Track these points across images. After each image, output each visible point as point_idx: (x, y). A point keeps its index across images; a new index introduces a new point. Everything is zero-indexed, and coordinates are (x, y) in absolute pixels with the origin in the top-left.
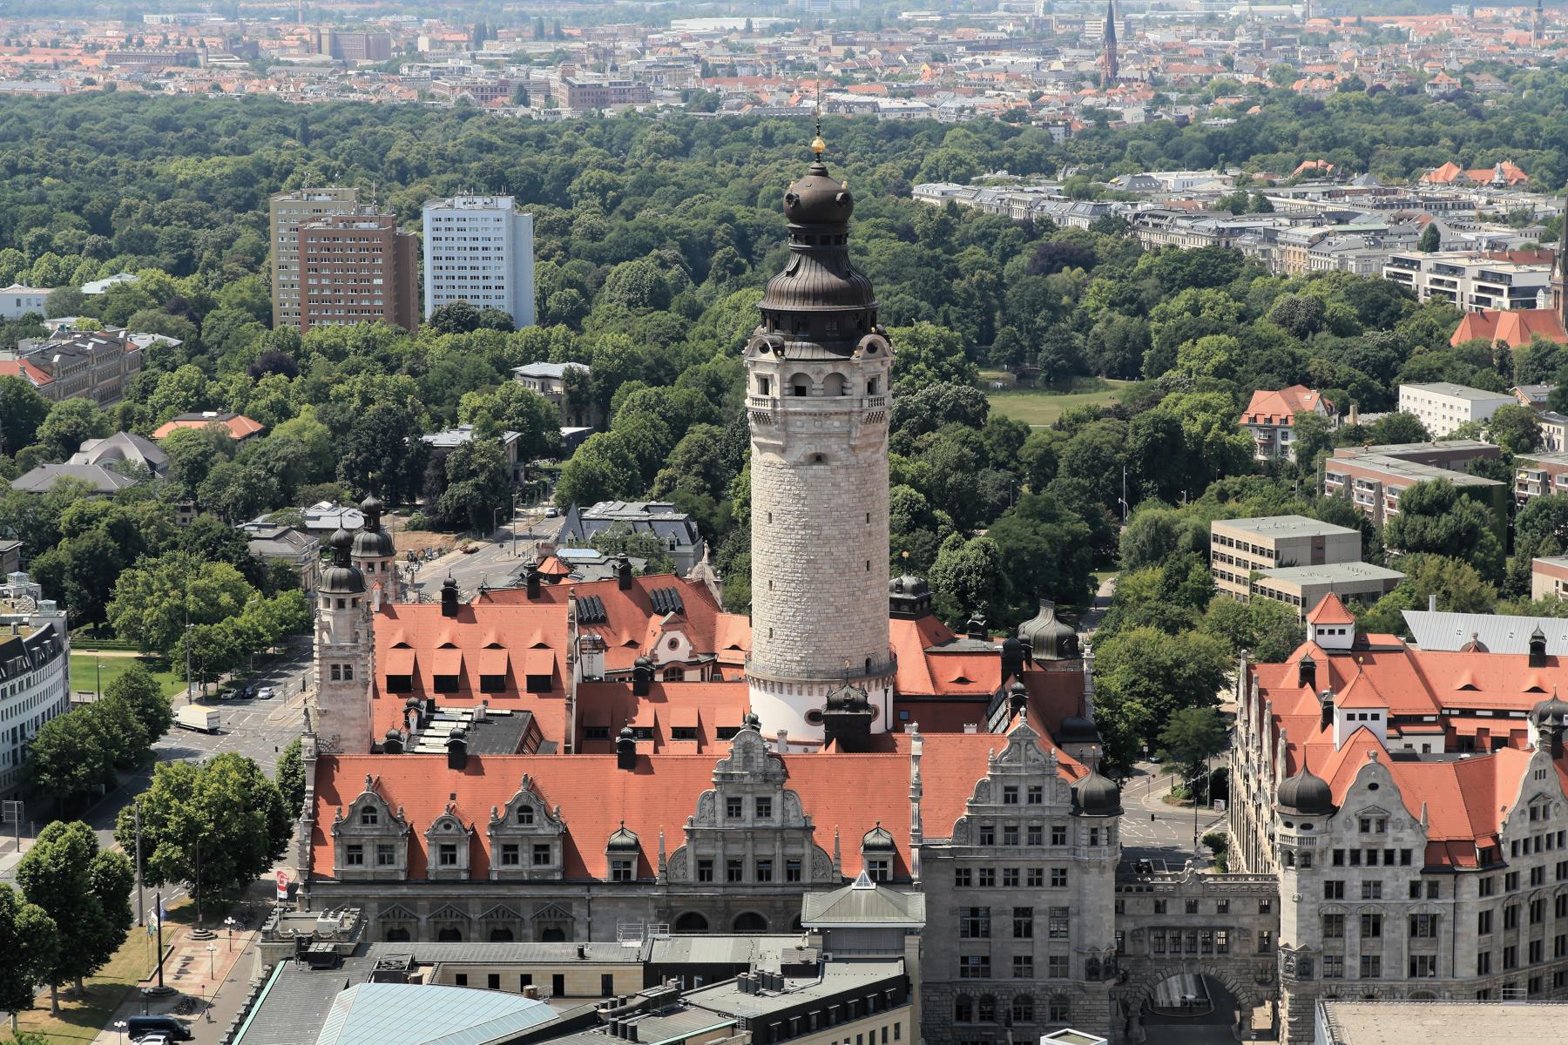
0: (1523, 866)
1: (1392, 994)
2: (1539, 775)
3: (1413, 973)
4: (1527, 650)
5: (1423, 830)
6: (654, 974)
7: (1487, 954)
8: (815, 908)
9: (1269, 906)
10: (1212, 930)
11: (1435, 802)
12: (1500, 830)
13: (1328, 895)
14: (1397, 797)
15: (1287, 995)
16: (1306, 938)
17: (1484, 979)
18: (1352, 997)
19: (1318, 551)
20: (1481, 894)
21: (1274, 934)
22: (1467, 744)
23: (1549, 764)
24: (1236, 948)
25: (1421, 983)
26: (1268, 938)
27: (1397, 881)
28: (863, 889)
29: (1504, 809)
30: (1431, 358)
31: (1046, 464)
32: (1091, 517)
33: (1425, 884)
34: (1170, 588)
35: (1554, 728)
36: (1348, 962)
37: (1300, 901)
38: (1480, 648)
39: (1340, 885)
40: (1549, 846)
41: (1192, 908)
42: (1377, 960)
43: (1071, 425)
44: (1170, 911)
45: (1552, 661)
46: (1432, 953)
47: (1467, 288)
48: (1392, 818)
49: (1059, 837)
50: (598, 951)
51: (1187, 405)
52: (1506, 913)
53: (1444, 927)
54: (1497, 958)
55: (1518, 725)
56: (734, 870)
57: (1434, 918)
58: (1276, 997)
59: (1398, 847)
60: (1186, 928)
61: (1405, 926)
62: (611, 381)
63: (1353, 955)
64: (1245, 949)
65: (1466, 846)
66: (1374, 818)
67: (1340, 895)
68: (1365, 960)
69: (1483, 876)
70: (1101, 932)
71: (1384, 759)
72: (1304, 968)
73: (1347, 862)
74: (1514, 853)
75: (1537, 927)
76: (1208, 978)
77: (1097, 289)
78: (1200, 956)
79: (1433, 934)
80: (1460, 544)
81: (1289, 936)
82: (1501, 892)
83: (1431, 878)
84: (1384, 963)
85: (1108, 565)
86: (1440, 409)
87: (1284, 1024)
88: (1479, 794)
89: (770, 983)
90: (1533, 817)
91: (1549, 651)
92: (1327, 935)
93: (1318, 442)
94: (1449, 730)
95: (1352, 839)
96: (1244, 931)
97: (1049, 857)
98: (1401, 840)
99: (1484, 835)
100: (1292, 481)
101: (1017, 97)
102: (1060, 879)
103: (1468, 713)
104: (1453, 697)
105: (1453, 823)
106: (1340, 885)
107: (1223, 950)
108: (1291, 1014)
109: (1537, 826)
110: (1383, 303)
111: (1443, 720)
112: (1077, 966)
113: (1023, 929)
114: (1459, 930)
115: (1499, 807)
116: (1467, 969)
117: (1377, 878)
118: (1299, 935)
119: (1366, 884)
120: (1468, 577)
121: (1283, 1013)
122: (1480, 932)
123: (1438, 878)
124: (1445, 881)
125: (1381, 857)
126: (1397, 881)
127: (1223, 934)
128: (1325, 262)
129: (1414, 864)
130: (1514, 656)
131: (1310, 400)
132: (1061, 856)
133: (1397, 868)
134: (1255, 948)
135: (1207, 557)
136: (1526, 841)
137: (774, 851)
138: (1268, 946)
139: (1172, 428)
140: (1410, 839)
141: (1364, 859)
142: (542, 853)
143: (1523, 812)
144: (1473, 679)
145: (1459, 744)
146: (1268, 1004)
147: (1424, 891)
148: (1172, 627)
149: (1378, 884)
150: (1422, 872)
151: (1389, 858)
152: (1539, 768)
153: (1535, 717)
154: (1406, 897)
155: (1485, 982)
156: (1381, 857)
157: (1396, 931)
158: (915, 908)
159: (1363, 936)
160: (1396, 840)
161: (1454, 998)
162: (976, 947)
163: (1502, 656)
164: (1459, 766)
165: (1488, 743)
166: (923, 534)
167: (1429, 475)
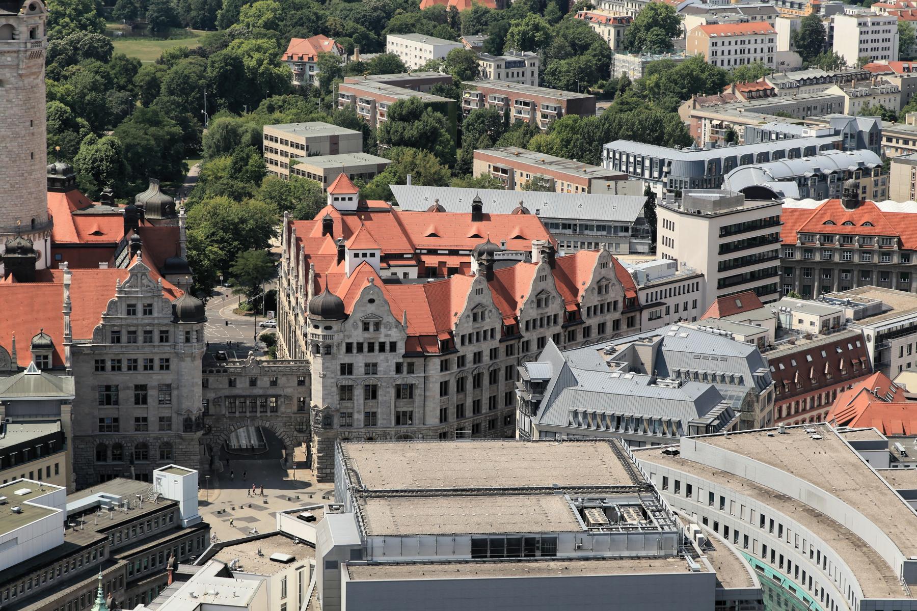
0: (468, 351)
1: (385, 437)
2: (478, 292)
3: (398, 422)
4: (470, 210)
5: (404, 329)
7: (446, 409)
9: (304, 381)
10: (267, 397)
11: (411, 310)
12: (453, 328)
13: (343, 373)
14: (387, 308)
15: (316, 439)
16: (329, 401)
17: (444, 425)
18: (359, 439)
20: (442, 370)
21: (307, 399)
22: (432, 272)
23: (485, 285)
24: (282, 409)
25: (403, 429)
26: (304, 402)
27: (386, 362)
29: (456, 314)
33: (405, 364)
35: (488, 261)
36: (356, 416)
37: (324, 377)
38: (440, 209)
39: (350, 366)
40: (485, 338)
41: (253, 383)
42: (374, 414)
44: (239, 385)
45: (487, 217)
46: (410, 409)
48: (384, 321)
52: (458, 382)
53: (418, 392)
54: (452, 411)
55: (465, 259)
57: (411, 386)
58: (309, 440)
59: (387, 341)
60: (249, 396)
61: (392, 392)
63: (359, 412)
64: (288, 409)
65: (432, 339)
66: (372, 321)
67: (350, 373)
68: (367, 415)
69: (443, 358)
71: (379, 283)
72: (327, 420)
73: (355, 351)
74: (463, 343)
75: (478, 391)
76: (265, 429)
78: (258, 414)
79: (411, 397)
81: (317, 400)
82: (455, 368)
83: (409, 360)
84: (379, 416)
87: (315, 457)
88: (440, 304)
90: (475, 319)
91: (484, 211)
92: (342, 399)
94: (420, 263)
95: (357, 336)
96: (288, 398)
98: (390, 335)
99: (443, 331)
103: (432, 252)
104: (422, 241)
105: (424, 325)
106: (350, 366)
107: (275, 410)
108: (319, 451)
109: (477, 325)
111: (417, 257)
114: (428, 394)
115: (453, 313)
116: (433, 419)
117: (374, 361)
118: (324, 400)
119: (367, 365)
121: (314, 450)
122: (441, 395)
123: (414, 360)
124: (418, 362)
125: (377, 347)
126: (386, 362)
127: (274, 400)
129: (398, 351)
130: (462, 214)
133: (388, 354)
134: (295, 408)
136: (470, 335)
138: (303, 407)
143: (468, 316)
144: (436, 229)
145: (426, 272)
146: (304, 445)
147: (405, 369)
149: (375, 365)
150: (403, 356)
152: (478, 287)
153: (476, 254)
154: (393, 373)
155: (445, 427)
156: (377, 347)
157: (386, 395)
159: (366, 399)
160: (387, 336)
161: (424, 438)
163: (454, 214)
164: (427, 287)
165: (445, 271)
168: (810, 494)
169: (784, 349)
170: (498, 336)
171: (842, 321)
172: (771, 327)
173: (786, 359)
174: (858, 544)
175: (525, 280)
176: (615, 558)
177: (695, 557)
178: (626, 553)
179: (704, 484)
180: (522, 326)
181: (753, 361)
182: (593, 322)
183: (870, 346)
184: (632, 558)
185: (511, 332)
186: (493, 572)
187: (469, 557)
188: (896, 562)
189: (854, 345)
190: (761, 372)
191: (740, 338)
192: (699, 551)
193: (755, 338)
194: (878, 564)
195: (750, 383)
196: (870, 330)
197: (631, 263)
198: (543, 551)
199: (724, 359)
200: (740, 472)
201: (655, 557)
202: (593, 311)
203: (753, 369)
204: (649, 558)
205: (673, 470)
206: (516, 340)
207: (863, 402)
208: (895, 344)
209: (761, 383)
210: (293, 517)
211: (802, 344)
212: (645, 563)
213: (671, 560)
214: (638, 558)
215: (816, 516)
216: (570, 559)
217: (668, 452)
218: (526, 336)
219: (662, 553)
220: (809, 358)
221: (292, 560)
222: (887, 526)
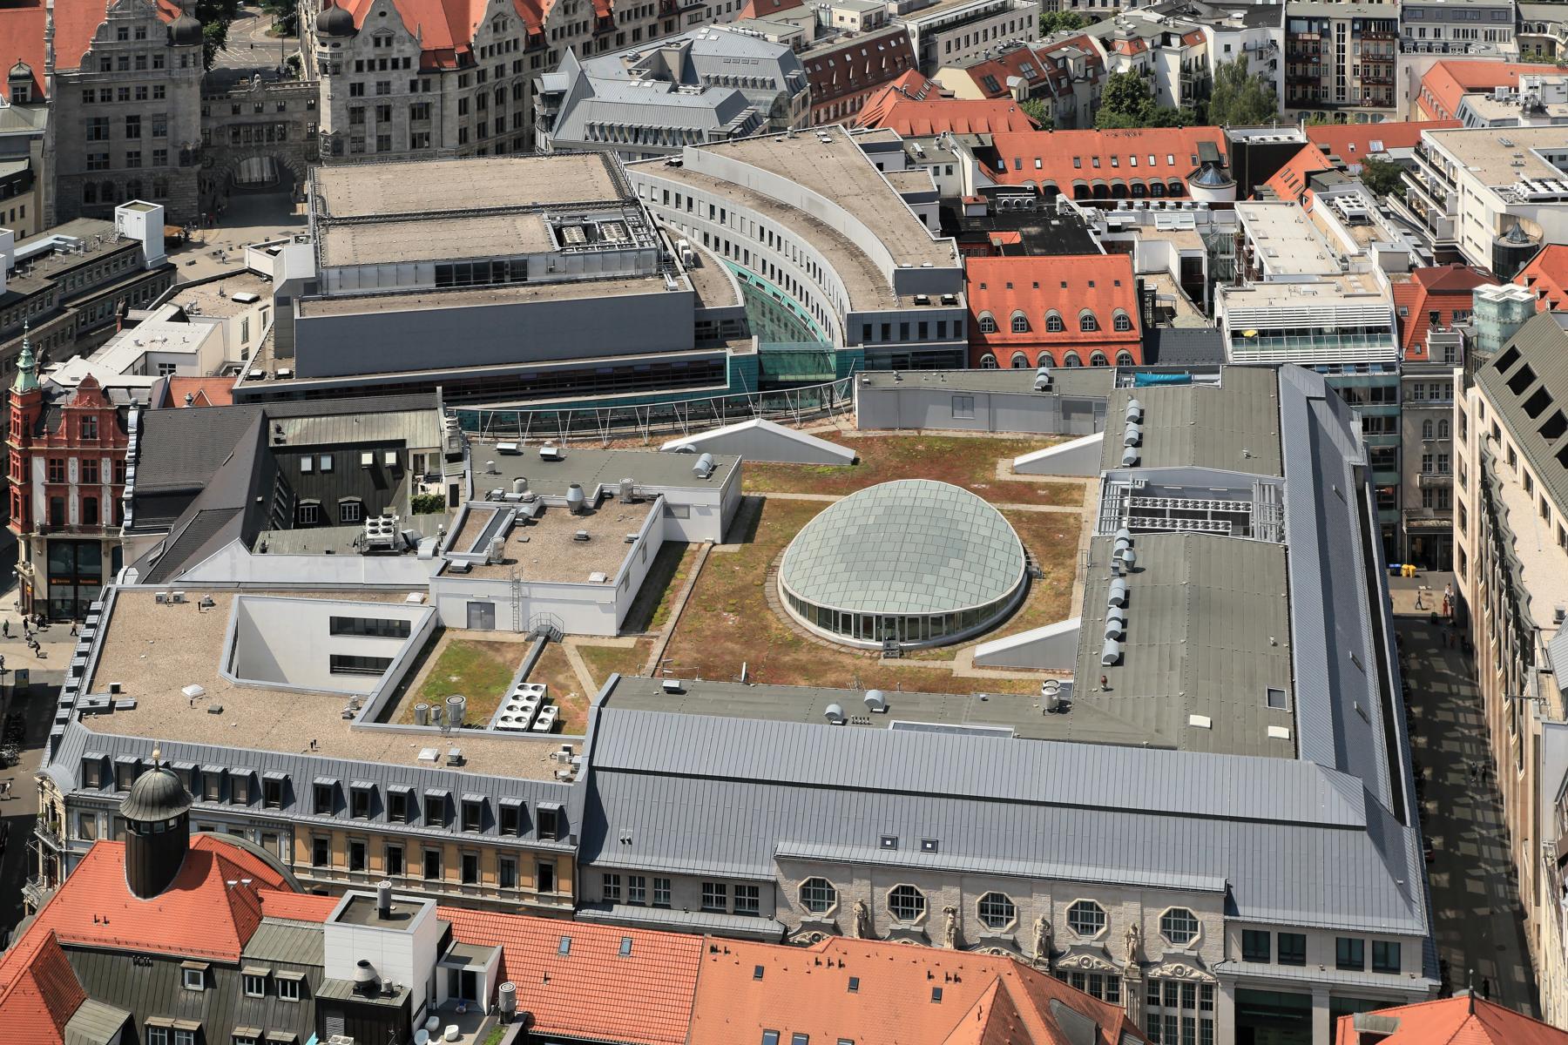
39: (361, 85)
40: (508, 50)
41: (259, 110)
44: (243, 112)
59: (401, 57)
65: (447, 53)
74: (483, 56)
106: (361, 85)
125: (389, 64)
133: (401, 71)
141: (377, 67)
151: (395, 64)
156: (389, 64)
168: (810, 201)
169: (822, 49)
170: (522, 47)
171: (885, 16)
172: (808, 27)
173: (823, 59)
174: (855, 253)
176: (590, 280)
177: (675, 274)
178: (602, 275)
179: (705, 196)
180: (548, 35)
181: (786, 63)
183: (915, 42)
184: (609, 279)
185: (536, 42)
186: (458, 301)
187: (433, 286)
189: (897, 42)
190: (794, 74)
191: (773, 38)
192: (681, 269)
193: (790, 38)
194: (872, 273)
195: (782, 86)
196: (913, 25)
198: (513, 275)
199: (756, 62)
200: (743, 182)
201: (633, 277)
203: (785, 70)
204: (627, 278)
205: (674, 183)
206: (541, 52)
207: (892, 100)
208: (941, 39)
209: (795, 86)
210: (263, 252)
211: (842, 42)
212: (620, 284)
213: (649, 279)
214: (615, 278)
215: (817, 226)
216: (542, 284)
217: (671, 164)
218: (553, 46)
219: (640, 272)
220: (848, 58)
221: (256, 299)
222: (884, 233)
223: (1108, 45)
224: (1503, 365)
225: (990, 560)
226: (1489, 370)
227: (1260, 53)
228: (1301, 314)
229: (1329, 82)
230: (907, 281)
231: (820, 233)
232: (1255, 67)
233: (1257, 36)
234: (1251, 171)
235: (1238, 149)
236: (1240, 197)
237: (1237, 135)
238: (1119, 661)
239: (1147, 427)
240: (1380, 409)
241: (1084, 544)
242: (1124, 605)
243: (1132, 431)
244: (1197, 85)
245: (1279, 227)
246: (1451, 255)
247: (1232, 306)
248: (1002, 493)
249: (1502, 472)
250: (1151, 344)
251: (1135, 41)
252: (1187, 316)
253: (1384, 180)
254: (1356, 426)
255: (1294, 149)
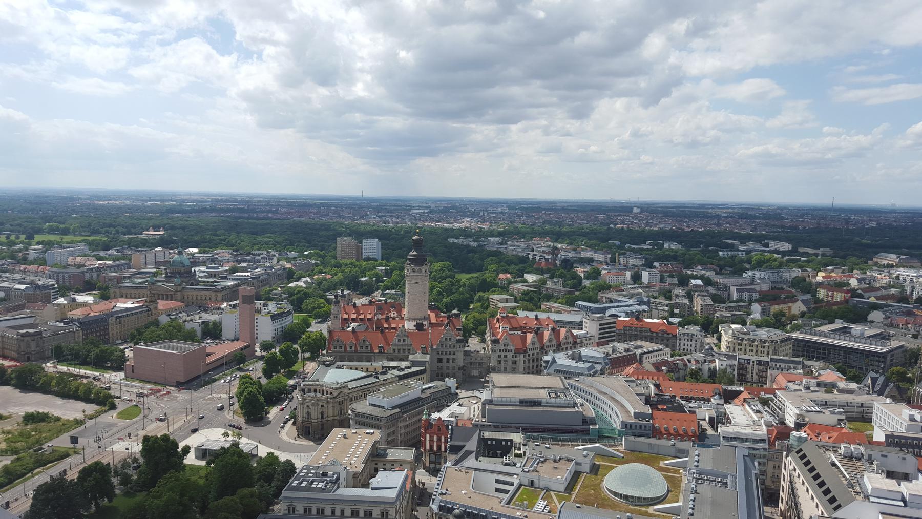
0: (531, 353)
6: (383, 367)
8: (411, 357)
19: (507, 301)
27: (510, 355)
28: (419, 354)
30: (530, 269)
31: (464, 285)
32: (470, 294)
34: (482, 306)
43: (469, 279)
47: (538, 258)
49: (454, 346)
50: (374, 364)
51: (488, 276)
56: (399, 351)
62: (392, 270)
70: (460, 361)
77: (477, 256)
80: (530, 300)
85: (472, 302)
86: (531, 278)
89: (403, 370)
93: (510, 283)
95: (503, 348)
97: (452, 350)
100: (504, 289)
101: (468, 225)
102: (454, 353)
110: (523, 260)
112: (457, 369)
113: (448, 361)
120: (531, 305)
126: (510, 355)
128: (514, 253)
131: (509, 276)
132: (454, 350)
135: (489, 302)
137: (406, 348)
139: (485, 280)
140: (512, 348)
142: (367, 347)
148: (481, 313)
158: (428, 357)
162: (440, 365)
166: (441, 297)
167: (526, 288)
174: (623, 406)
175: (547, 334)
182: (564, 347)
188: (632, 411)
194: (628, 412)
197: (575, 332)
202: (564, 344)
206: (543, 350)
215: (613, 399)
223: (689, 361)
224: (798, 452)
225: (657, 485)
226: (794, 453)
227: (731, 366)
228: (742, 434)
229: (749, 376)
230: (637, 415)
231: (618, 400)
232: (729, 370)
233: (730, 362)
234: (729, 397)
235: (725, 390)
236: (725, 402)
237: (724, 387)
238: (692, 515)
239: (700, 458)
240: (762, 460)
241: (683, 485)
242: (694, 501)
243: (696, 458)
244: (713, 373)
245: (734, 410)
246: (782, 422)
247: (722, 430)
248: (661, 469)
249: (796, 479)
250: (701, 438)
251: (697, 361)
252: (710, 431)
253: (765, 402)
254: (756, 464)
255: (741, 392)
